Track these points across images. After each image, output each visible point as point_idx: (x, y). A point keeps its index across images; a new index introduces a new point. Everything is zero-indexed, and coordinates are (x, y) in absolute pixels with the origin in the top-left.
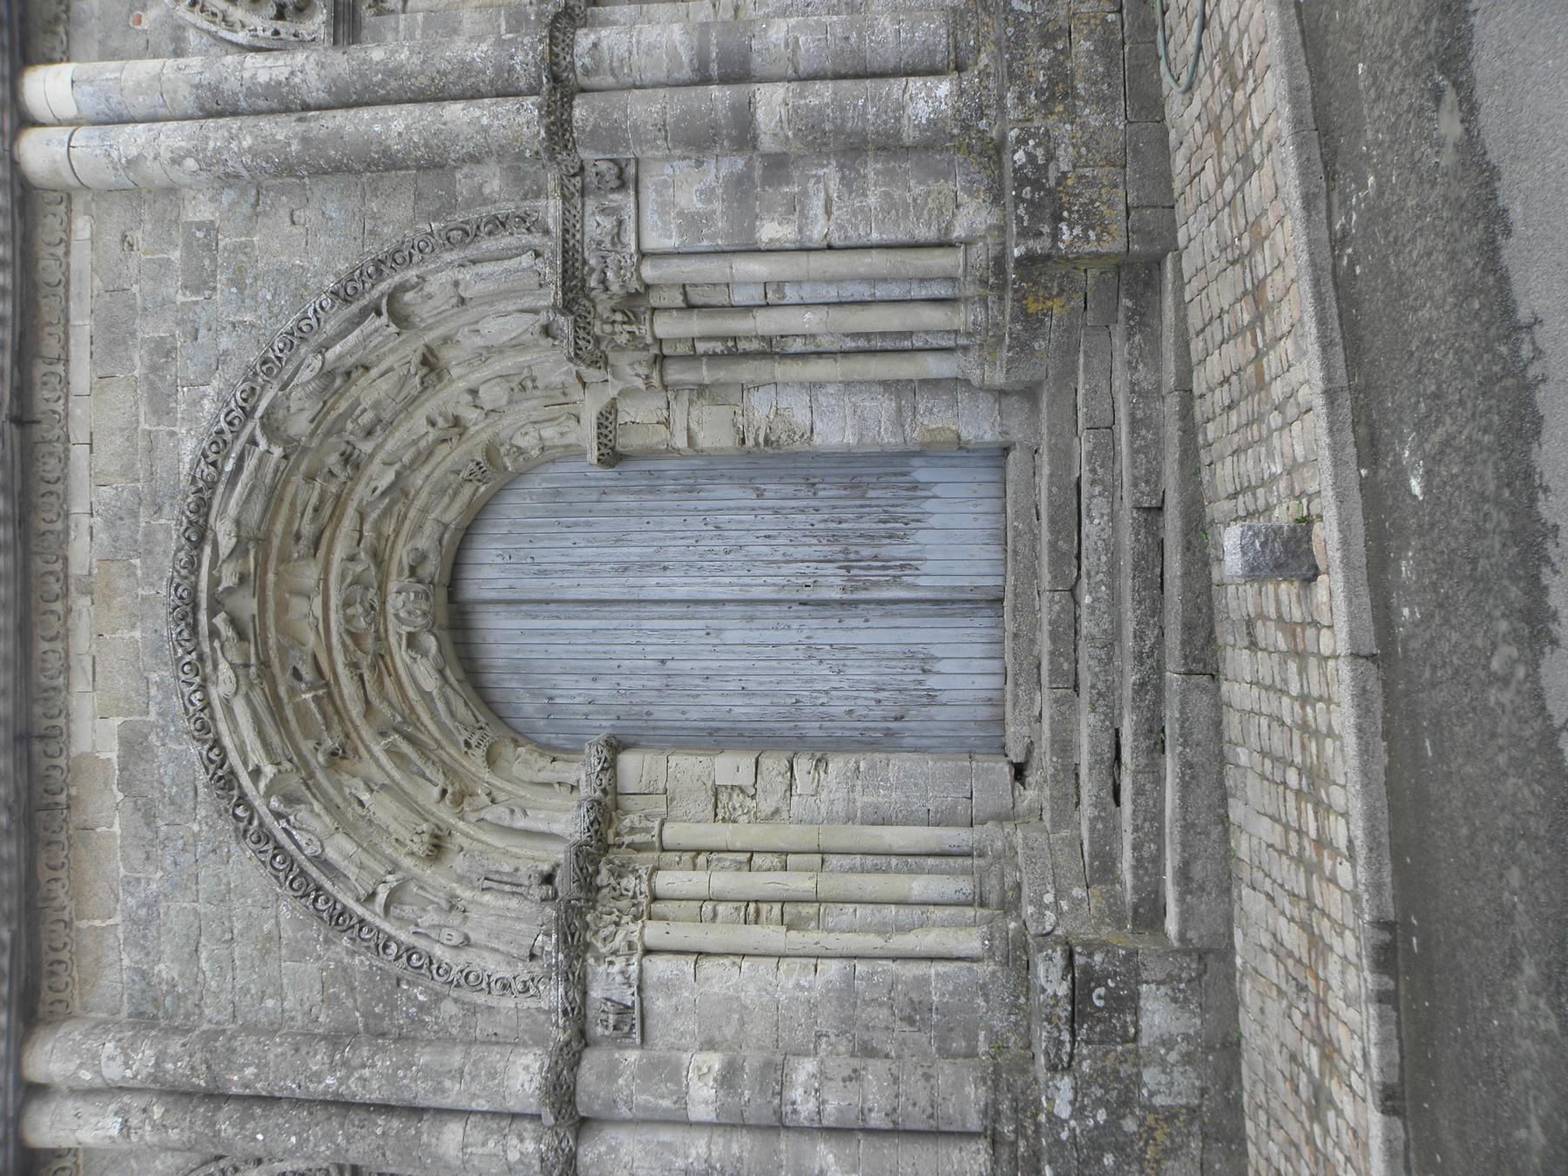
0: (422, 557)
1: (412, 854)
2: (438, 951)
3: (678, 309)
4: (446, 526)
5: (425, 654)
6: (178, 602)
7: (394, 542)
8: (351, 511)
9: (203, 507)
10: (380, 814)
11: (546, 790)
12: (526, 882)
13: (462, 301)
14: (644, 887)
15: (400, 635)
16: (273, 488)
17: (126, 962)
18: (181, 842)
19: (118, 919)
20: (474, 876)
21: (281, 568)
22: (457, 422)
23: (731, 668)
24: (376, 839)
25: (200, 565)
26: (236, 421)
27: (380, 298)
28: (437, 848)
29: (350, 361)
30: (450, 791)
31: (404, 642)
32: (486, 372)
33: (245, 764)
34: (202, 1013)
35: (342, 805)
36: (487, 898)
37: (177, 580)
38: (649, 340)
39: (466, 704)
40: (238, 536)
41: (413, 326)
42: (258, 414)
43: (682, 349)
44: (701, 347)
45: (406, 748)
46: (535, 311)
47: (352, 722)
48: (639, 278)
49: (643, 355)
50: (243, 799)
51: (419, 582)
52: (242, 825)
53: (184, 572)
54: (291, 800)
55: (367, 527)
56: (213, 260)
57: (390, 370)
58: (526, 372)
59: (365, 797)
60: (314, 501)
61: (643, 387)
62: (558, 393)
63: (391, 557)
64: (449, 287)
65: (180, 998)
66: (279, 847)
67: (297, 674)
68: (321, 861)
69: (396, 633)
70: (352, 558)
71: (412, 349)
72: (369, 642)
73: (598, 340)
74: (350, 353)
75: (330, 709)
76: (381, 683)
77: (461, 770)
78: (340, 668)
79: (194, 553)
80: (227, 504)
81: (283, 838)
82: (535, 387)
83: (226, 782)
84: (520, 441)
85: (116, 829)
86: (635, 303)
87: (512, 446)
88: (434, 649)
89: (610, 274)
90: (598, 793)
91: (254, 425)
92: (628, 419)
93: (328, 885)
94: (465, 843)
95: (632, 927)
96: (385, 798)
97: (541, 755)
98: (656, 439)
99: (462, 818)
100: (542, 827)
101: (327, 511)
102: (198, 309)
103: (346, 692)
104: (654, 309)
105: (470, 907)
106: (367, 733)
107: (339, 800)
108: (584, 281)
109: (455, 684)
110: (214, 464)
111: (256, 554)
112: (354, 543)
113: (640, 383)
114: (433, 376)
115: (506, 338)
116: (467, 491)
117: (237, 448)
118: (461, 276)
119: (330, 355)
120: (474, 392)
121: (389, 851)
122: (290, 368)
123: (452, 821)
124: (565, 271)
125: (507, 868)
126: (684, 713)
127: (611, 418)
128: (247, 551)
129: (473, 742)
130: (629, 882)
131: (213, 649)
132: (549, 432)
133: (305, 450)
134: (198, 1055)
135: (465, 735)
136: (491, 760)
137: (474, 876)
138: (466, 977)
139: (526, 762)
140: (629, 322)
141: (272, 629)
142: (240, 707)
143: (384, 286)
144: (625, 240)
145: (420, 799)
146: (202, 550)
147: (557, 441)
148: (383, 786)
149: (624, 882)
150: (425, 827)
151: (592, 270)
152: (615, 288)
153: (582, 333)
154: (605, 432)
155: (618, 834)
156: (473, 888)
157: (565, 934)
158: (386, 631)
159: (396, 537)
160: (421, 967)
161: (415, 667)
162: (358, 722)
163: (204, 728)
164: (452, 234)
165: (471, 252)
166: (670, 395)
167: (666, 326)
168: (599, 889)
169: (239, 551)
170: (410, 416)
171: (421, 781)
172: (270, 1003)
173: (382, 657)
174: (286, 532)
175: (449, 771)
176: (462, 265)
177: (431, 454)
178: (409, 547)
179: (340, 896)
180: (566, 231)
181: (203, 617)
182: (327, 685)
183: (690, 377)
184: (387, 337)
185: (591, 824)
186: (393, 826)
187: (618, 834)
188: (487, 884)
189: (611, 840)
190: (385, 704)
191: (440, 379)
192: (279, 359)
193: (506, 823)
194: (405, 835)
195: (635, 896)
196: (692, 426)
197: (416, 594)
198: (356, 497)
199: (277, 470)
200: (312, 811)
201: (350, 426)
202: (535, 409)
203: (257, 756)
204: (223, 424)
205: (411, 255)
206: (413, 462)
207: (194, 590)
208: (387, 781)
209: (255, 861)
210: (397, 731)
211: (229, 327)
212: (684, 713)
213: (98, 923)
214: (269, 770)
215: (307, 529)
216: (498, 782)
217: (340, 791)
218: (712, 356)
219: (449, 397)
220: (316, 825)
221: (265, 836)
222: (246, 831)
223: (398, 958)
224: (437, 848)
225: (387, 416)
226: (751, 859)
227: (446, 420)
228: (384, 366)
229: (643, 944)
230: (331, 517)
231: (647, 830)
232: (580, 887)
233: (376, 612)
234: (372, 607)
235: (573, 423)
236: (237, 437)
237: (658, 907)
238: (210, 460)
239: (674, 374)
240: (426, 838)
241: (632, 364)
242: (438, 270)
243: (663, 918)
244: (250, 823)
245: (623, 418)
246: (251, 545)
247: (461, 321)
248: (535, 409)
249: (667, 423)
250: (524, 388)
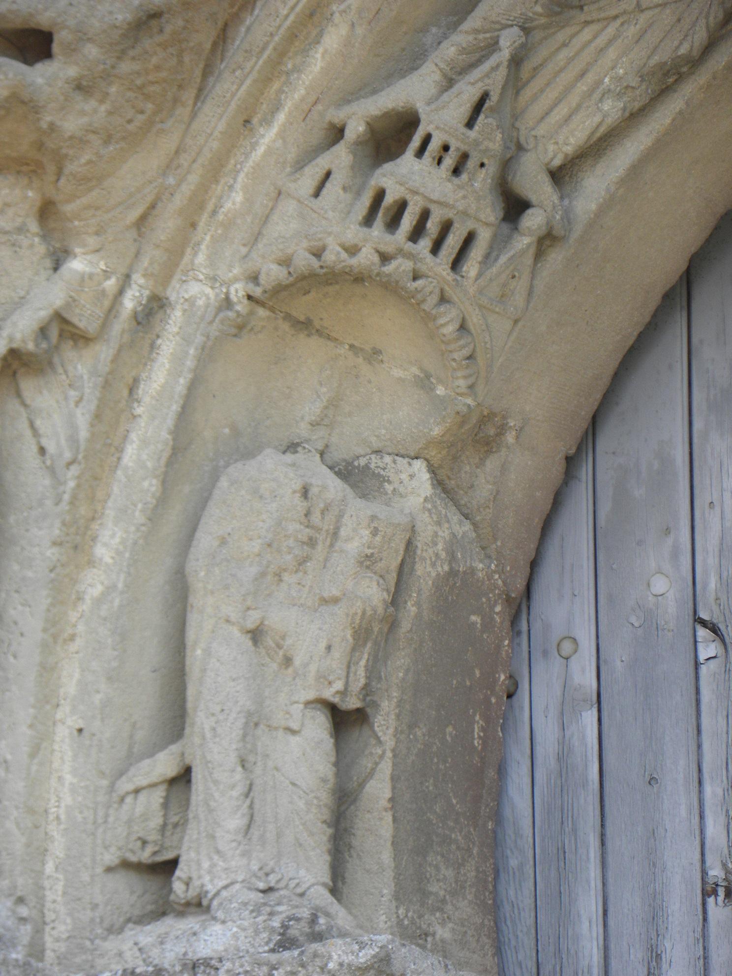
30: (43, 77)
97: (374, 636)
129: (409, 176)
135: (443, 119)
139: (317, 535)
216: (163, 376)
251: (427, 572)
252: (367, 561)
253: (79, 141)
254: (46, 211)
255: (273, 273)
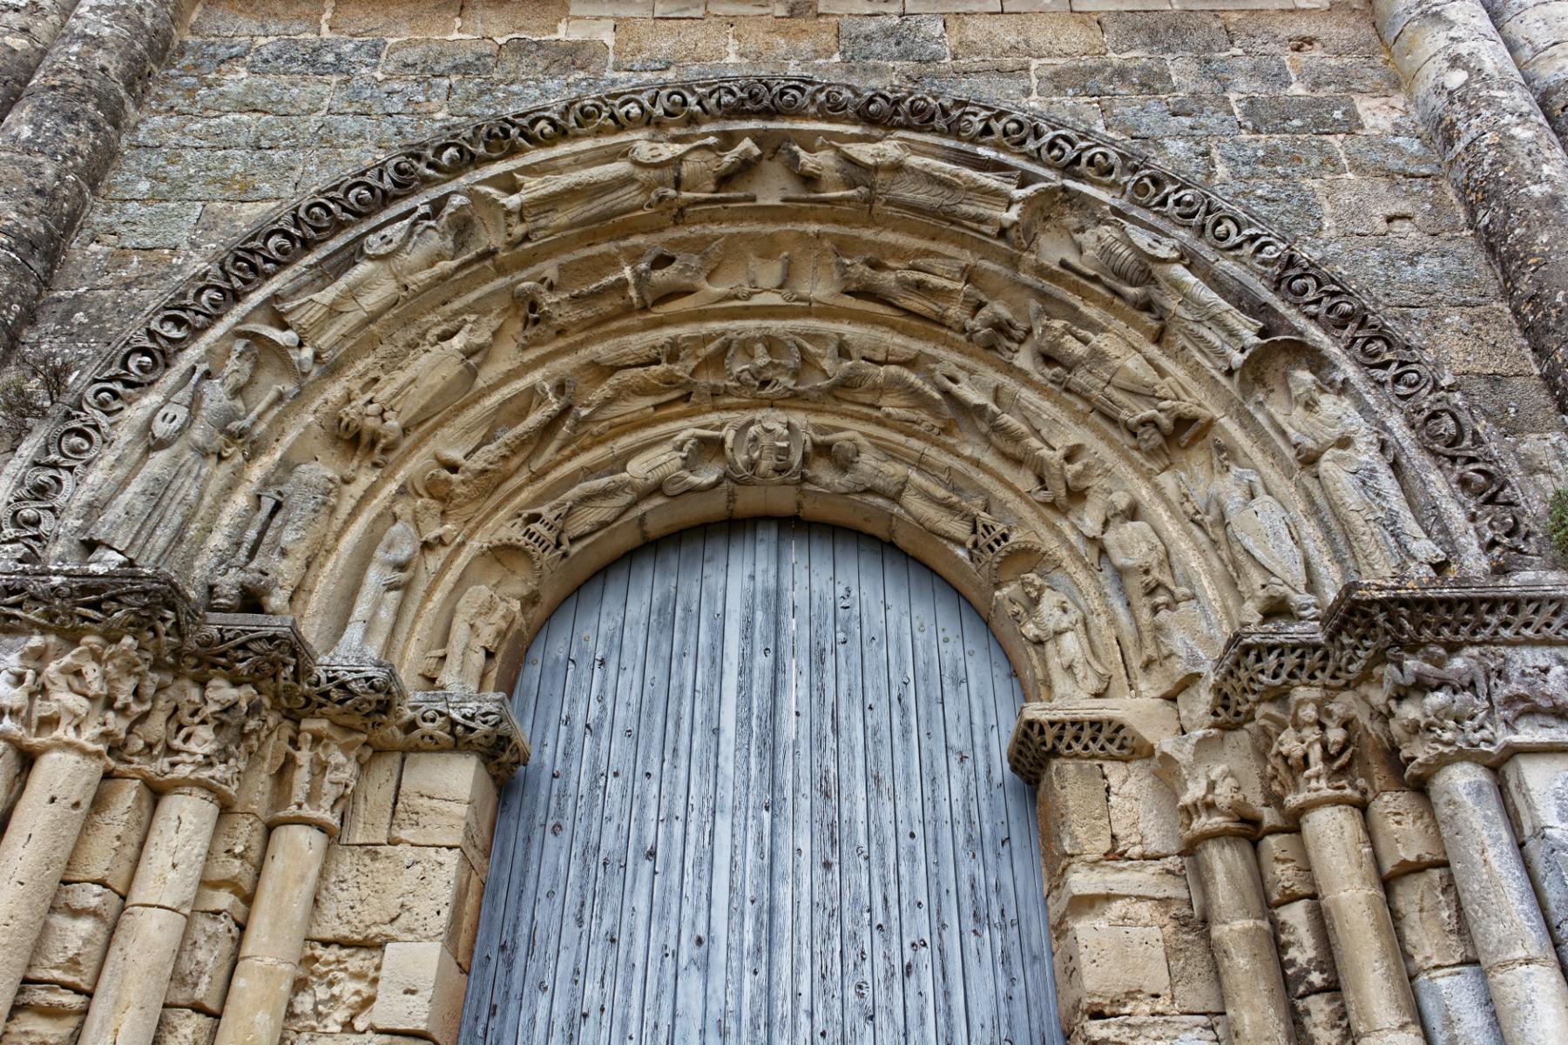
0: (844, 463)
1: (349, 399)
2: (152, 399)
3: (1376, 859)
4: (895, 498)
5: (688, 464)
6: (776, 89)
7: (868, 419)
8: (916, 346)
9: (922, 119)
10: (424, 358)
11: (437, 639)
12: (254, 565)
13: (1310, 460)
14: (183, 771)
15: (720, 428)
16: (951, 217)
17: (262, 41)
18: (421, 98)
19: (326, 33)
20: (285, 488)
21: (827, 244)
22: (1077, 495)
23: (628, 991)
24: (382, 351)
25: (831, 120)
26: (1056, 152)
27: (1293, 329)
28: (352, 440)
29: (1173, 304)
30: (454, 476)
31: (708, 433)
32: (1172, 529)
33: (526, 170)
34: (158, 113)
35: (448, 308)
36: (241, 500)
37: (810, 89)
38: (1293, 800)
39: (603, 525)
40: (876, 168)
41: (1246, 392)
42: (1070, 183)
43: (1283, 875)
44: (1296, 916)
45: (535, 418)
46: (1311, 586)
47: (582, 344)
48: (1443, 761)
49: (1255, 798)
50: (475, 162)
51: (805, 459)
52: (429, 153)
53: (822, 97)
54: (462, 227)
55: (893, 369)
56: (1302, 129)
57: (1162, 373)
58: (1181, 591)
59: (457, 342)
60: (934, 280)
61: (1186, 799)
62: (1151, 651)
63: (845, 415)
64: (1336, 432)
65: (191, 91)
66: (387, 199)
67: (662, 261)
68: (353, 254)
69: (725, 423)
70: (843, 351)
71: (1199, 401)
72: (707, 379)
73: (1279, 696)
74: (1188, 299)
75: (606, 306)
76: (643, 391)
77: (491, 503)
78: (670, 332)
79: (850, 111)
80: (924, 154)
81: (404, 206)
82: (1155, 610)
83: (502, 139)
84: (1049, 601)
85: (456, 36)
86: (1383, 767)
87: (1040, 590)
88: (694, 479)
89: (1438, 698)
90: (408, 714)
91: (1053, 179)
92: (1114, 780)
93: (311, 259)
94: (356, 490)
95: (91, 731)
96: (452, 369)
97: (501, 635)
98: (1080, 832)
99: (402, 491)
100: (361, 609)
101: (916, 303)
102: (1222, 115)
103: (633, 338)
104: (1362, 807)
105: (226, 468)
106: (565, 364)
107: (457, 304)
108: (1414, 648)
109: (637, 512)
110: (988, 130)
111: (849, 199)
112: (866, 353)
113: (1194, 791)
114: (1157, 439)
115: (1249, 543)
116: (959, 529)
117: (1013, 160)
118: (1361, 446)
119: (1179, 271)
120: (1133, 512)
121: (360, 366)
122: (1151, 218)
123: (401, 475)
124: (1429, 604)
125: (288, 537)
126: (551, 894)
127: (1113, 749)
128: (852, 185)
129: (536, 527)
130: (204, 741)
131: (706, 135)
132: (1071, 644)
133: (1014, 262)
134: (79, 80)
136: (503, 553)
137: (285, 488)
138: (80, 433)
140: (1328, 758)
141: (734, 230)
142: (620, 167)
143: (1315, 334)
144: (1522, 725)
145: (446, 431)
146: (855, 123)
147: (1055, 663)
148: (472, 373)
149: (205, 733)
150: (394, 423)
151: (1439, 663)
152: (1409, 711)
153: (1291, 661)
154: (1086, 735)
155: (317, 739)
156: (266, 483)
157: (97, 591)
158: (728, 408)
159: (879, 423)
160: (124, 365)
161: (667, 447)
162: (583, 352)
163: (586, 115)
164: (1446, 418)
165: (1416, 458)
166: (1173, 862)
167: (1332, 831)
168: (203, 684)
169: (854, 171)
170: (1080, 419)
171: (477, 437)
172: (144, 186)
173: (686, 398)
174: (881, 246)
175: (489, 482)
176: (1383, 447)
177: (1018, 462)
178: (862, 440)
179: (288, 273)
180: (1515, 605)
181: (753, 124)
182: (645, 309)
183: (1224, 892)
184: (1221, 355)
185: (343, 686)
186: (401, 377)
187: (317, 739)
188: (267, 504)
189: (309, 725)
190: (609, 393)
191: (1151, 454)
192: (1163, 202)
193: (379, 554)
194: (384, 392)
195: (170, 750)
196: (1117, 908)
197: (786, 451)
198: (941, 352)
199: (981, 220)
200: (440, 256)
201: (1058, 324)
202: (1112, 622)
203: (535, 187)
204: (1050, 135)
205: (1385, 365)
206: (1003, 430)
207: (799, 114)
208: (480, 383)
209: (368, 162)
210: (565, 411)
211: (1201, 149)
212: (551, 894)
213: (328, 15)
214: (513, 201)
215: (887, 279)
217: (469, 309)
218: (1276, 942)
219: (1120, 478)
220: (415, 255)
221: (406, 183)
222: (418, 158)
223: (151, 334)
224: (352, 440)
225: (1080, 378)
226: (198, 1008)
227: (1077, 476)
228: (1165, 363)
229: (46, 749)
230: (909, 313)
231: (312, 796)
232: (208, 643)
233: (759, 392)
234: (765, 383)
235: (1093, 684)
236: (1030, 158)
237: (128, 795)
238: (993, 123)
239: (1223, 862)
240: (372, 423)
241: (1230, 774)
242: (1364, 409)
243: (99, 803)
244: (430, 165)
245: (1115, 773)
246: (863, 189)
247: (1266, 470)
248: (1112, 622)
249: (1115, 854)
250: (1151, 591)
251: (516, 627)
252: (504, 617)
253: (459, 496)
254: (443, 513)
255: (496, 542)
